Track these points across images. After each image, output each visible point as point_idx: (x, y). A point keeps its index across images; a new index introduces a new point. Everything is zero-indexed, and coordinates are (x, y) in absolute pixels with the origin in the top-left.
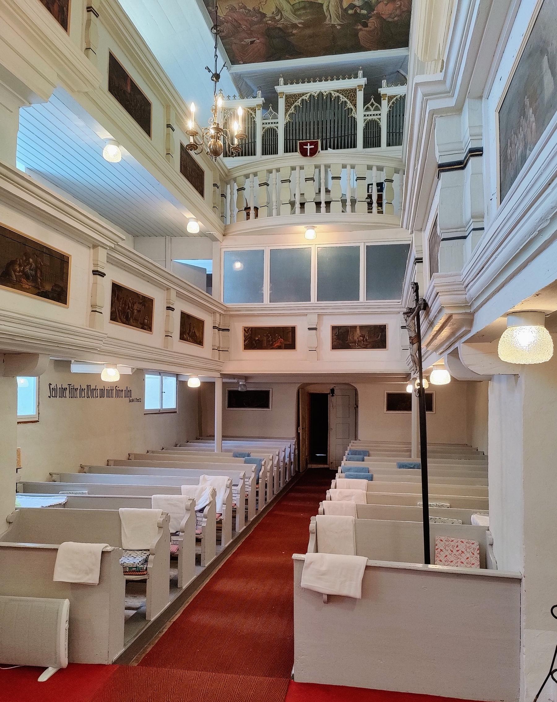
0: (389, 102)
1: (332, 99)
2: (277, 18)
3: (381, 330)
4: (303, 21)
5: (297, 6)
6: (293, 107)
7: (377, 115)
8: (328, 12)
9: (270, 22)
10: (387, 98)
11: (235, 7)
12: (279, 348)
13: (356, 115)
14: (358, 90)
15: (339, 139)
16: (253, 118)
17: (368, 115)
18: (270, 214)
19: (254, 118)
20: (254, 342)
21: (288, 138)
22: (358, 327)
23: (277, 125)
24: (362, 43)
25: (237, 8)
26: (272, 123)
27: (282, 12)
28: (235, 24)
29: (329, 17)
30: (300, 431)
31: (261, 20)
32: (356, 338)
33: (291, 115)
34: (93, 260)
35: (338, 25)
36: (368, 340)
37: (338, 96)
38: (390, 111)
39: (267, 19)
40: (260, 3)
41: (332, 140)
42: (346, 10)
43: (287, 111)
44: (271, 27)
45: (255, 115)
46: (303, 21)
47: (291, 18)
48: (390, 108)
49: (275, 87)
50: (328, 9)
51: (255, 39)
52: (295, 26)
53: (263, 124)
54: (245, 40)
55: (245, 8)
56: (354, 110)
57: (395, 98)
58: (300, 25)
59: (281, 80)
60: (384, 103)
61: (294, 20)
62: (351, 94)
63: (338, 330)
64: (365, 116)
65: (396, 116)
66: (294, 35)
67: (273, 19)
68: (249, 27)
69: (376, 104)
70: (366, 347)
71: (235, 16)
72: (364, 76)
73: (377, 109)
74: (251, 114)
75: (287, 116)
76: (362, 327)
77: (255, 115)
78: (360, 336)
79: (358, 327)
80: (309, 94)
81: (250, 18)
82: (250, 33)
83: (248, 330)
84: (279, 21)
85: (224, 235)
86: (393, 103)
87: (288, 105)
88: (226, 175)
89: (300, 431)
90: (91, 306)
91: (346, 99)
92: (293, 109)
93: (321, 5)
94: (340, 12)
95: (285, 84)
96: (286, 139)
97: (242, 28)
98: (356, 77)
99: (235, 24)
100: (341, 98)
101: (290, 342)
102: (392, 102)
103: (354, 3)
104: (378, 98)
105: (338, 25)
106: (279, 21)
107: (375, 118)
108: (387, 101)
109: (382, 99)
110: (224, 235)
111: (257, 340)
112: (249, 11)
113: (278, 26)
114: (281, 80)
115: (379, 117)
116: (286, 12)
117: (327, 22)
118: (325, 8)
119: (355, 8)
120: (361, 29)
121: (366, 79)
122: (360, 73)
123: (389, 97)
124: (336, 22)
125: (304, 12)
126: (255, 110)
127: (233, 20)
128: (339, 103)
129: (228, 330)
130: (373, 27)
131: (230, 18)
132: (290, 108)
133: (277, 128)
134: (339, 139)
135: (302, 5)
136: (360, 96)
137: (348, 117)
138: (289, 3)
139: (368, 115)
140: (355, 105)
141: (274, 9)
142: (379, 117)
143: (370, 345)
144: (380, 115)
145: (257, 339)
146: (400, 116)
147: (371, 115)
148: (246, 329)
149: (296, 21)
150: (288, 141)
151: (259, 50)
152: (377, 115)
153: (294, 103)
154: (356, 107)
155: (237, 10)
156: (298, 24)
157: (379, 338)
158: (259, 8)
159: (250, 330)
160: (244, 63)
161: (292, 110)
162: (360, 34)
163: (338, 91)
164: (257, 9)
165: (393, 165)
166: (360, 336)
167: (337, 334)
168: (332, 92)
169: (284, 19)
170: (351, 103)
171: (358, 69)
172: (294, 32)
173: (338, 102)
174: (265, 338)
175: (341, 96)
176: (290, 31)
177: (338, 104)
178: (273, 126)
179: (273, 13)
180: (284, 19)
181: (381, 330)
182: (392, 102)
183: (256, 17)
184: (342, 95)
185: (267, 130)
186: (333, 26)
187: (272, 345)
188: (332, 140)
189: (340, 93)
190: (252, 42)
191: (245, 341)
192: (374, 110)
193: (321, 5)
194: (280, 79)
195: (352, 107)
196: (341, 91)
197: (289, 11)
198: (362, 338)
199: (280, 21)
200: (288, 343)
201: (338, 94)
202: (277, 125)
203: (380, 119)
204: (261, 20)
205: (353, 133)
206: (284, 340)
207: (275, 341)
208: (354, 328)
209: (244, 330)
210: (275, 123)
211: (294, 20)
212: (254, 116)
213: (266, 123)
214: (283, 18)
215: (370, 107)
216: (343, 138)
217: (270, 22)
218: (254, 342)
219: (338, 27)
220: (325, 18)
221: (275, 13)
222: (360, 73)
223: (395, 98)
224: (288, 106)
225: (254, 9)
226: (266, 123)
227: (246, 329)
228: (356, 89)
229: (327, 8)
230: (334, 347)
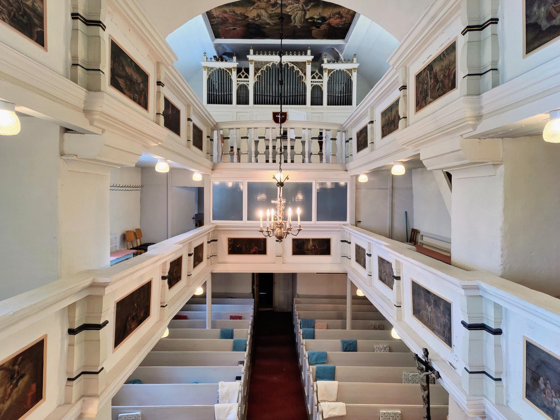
0: (328, 73)
1: (289, 68)
3: (327, 242)
6: (260, 71)
7: (320, 82)
9: (251, 21)
10: (327, 71)
12: (255, 253)
13: (305, 82)
14: (307, 64)
15: (294, 98)
16: (229, 76)
17: (314, 82)
18: (250, 161)
19: (231, 76)
20: (236, 249)
21: (256, 94)
22: (311, 240)
23: (248, 83)
24: (313, 35)
26: (244, 81)
28: (224, 19)
29: (294, 22)
30: (255, 288)
32: (309, 247)
33: (259, 77)
34: (162, 269)
35: (300, 26)
36: (318, 249)
37: (293, 67)
38: (329, 80)
39: (248, 19)
40: (246, 11)
41: (289, 98)
42: (307, 19)
43: (255, 74)
45: (232, 74)
48: (329, 78)
49: (247, 56)
50: (294, 18)
52: (268, 24)
53: (238, 81)
56: (304, 78)
57: (332, 72)
58: (271, 24)
59: (251, 51)
60: (325, 74)
62: (302, 65)
63: (297, 242)
64: (312, 82)
65: (333, 84)
66: (266, 28)
67: (253, 19)
68: (234, 21)
69: (320, 74)
70: (316, 254)
71: (226, 15)
72: (311, 55)
73: (320, 78)
74: (228, 73)
75: (256, 77)
76: (314, 240)
77: (232, 74)
78: (312, 246)
79: (311, 240)
80: (272, 63)
82: (234, 24)
83: (231, 240)
85: (212, 170)
86: (331, 75)
87: (257, 70)
88: (215, 126)
89: (255, 288)
90: (161, 303)
91: (298, 69)
92: (260, 73)
95: (255, 54)
96: (255, 95)
98: (306, 54)
100: (295, 68)
101: (262, 249)
102: (331, 74)
103: (314, 17)
104: (321, 70)
105: (300, 26)
107: (319, 84)
108: (327, 73)
109: (324, 71)
110: (212, 170)
111: (238, 247)
112: (237, 14)
114: (251, 51)
115: (322, 83)
117: (292, 24)
118: (292, 17)
120: (315, 29)
121: (313, 57)
122: (309, 52)
123: (328, 70)
126: (232, 70)
128: (294, 72)
129: (216, 240)
130: (323, 29)
131: (221, 16)
132: (258, 72)
133: (248, 85)
134: (294, 98)
136: (309, 68)
137: (300, 82)
138: (268, 13)
139: (314, 82)
140: (305, 74)
142: (322, 83)
143: (319, 252)
144: (322, 82)
145: (238, 246)
146: (336, 83)
147: (316, 82)
148: (230, 240)
149: (270, 22)
150: (256, 96)
152: (320, 82)
153: (260, 69)
154: (305, 76)
155: (228, 13)
157: (326, 247)
159: (233, 240)
160: (224, 38)
161: (259, 73)
162: (313, 31)
163: (292, 63)
165: (336, 128)
166: (312, 246)
167: (296, 244)
168: (289, 63)
170: (302, 72)
171: (307, 49)
172: (267, 26)
173: (293, 71)
174: (244, 246)
175: (295, 67)
177: (293, 72)
178: (245, 83)
181: (327, 242)
182: (331, 74)
184: (296, 66)
185: (240, 86)
187: (249, 251)
188: (289, 98)
189: (294, 64)
191: (229, 248)
192: (318, 78)
194: (250, 50)
195: (303, 75)
196: (295, 63)
198: (313, 247)
200: (261, 250)
201: (293, 65)
202: (248, 83)
203: (322, 85)
205: (303, 94)
206: (257, 247)
207: (251, 249)
208: (308, 240)
209: (228, 240)
210: (246, 81)
212: (231, 75)
213: (240, 81)
215: (315, 76)
216: (296, 97)
217: (251, 21)
218: (236, 249)
220: (291, 22)
222: (309, 52)
223: (332, 72)
224: (257, 70)
226: (240, 81)
227: (230, 240)
228: (305, 63)
230: (295, 253)
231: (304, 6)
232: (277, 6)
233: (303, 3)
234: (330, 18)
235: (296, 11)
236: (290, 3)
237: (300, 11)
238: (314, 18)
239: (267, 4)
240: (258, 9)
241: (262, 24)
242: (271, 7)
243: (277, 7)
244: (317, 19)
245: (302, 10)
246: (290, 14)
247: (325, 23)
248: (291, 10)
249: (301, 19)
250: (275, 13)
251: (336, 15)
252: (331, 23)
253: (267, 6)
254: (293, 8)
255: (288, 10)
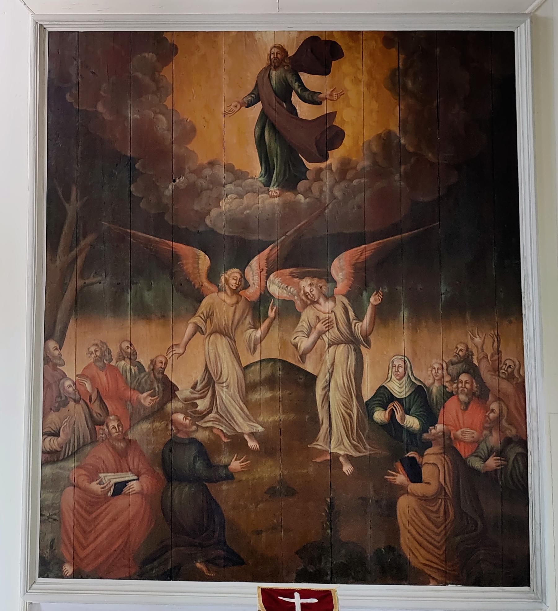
2: (202, 405)
4: (261, 429)
5: (254, 375)
8: (326, 407)
9: (180, 417)
11: (110, 353)
25: (115, 352)
27: (216, 385)
31: (162, 406)
35: (349, 458)
39: (176, 404)
40: (172, 346)
44: (179, 435)
46: (261, 429)
47: (235, 413)
50: (326, 397)
51: (130, 476)
54: (102, 475)
55: (132, 357)
58: (252, 444)
61: (240, 420)
66: (230, 477)
71: (103, 378)
81: (135, 395)
84: (202, 416)
93: (312, 378)
94: (355, 411)
97: (108, 427)
99: (96, 408)
105: (349, 458)
106: (202, 416)
113: (201, 435)
116: (225, 389)
117: (320, 444)
119: (390, 406)
124: (342, 447)
125: (268, 395)
127: (94, 397)
131: (88, 387)
135: (267, 372)
141: (198, 375)
151: (129, 524)
155: (113, 363)
156: (246, 437)
158: (166, 363)
164: (160, 365)
169: (217, 412)
172: (235, 465)
176: (224, 460)
179: (194, 387)
180: (217, 412)
183: (151, 395)
186: (334, 460)
190: (120, 488)
193: (312, 378)
197: (234, 389)
199: (207, 418)
204: (162, 406)
211: (240, 420)
214: (214, 410)
217: (180, 417)
219: (347, 468)
221: (199, 387)
225: (153, 362)
229: (324, 392)
231: (352, 314)
232: (267, 316)
233: (346, 296)
234: (447, 395)
235: (330, 346)
236: (306, 294)
237: (342, 346)
238: (392, 398)
239: (237, 302)
240: (210, 334)
241: (216, 442)
242: (249, 319)
243: (267, 322)
244: (400, 401)
245: (347, 342)
246: (309, 367)
247: (436, 438)
248: (313, 336)
249: (347, 406)
250: (261, 361)
251: (464, 377)
252: (456, 438)
253: (237, 317)
254: (319, 326)
255: (304, 343)
